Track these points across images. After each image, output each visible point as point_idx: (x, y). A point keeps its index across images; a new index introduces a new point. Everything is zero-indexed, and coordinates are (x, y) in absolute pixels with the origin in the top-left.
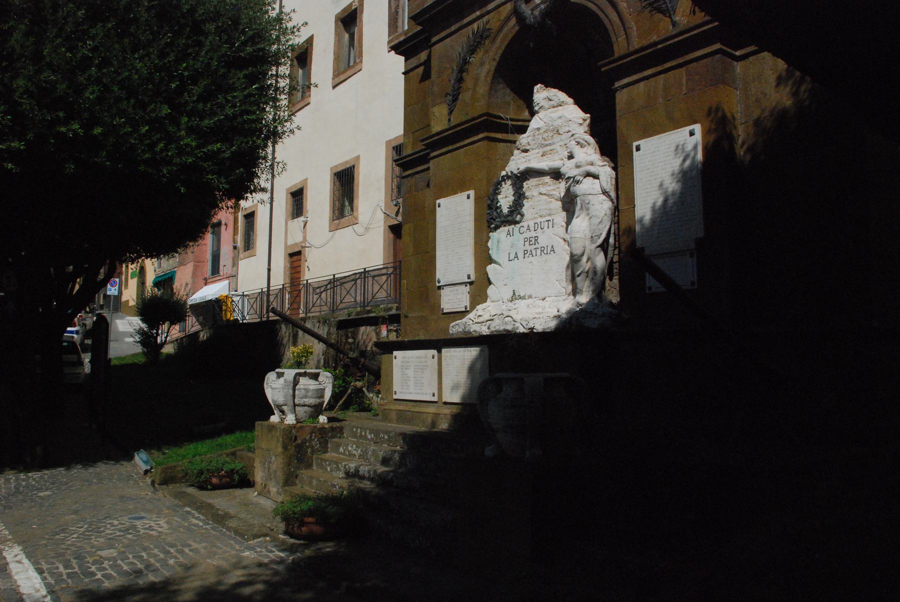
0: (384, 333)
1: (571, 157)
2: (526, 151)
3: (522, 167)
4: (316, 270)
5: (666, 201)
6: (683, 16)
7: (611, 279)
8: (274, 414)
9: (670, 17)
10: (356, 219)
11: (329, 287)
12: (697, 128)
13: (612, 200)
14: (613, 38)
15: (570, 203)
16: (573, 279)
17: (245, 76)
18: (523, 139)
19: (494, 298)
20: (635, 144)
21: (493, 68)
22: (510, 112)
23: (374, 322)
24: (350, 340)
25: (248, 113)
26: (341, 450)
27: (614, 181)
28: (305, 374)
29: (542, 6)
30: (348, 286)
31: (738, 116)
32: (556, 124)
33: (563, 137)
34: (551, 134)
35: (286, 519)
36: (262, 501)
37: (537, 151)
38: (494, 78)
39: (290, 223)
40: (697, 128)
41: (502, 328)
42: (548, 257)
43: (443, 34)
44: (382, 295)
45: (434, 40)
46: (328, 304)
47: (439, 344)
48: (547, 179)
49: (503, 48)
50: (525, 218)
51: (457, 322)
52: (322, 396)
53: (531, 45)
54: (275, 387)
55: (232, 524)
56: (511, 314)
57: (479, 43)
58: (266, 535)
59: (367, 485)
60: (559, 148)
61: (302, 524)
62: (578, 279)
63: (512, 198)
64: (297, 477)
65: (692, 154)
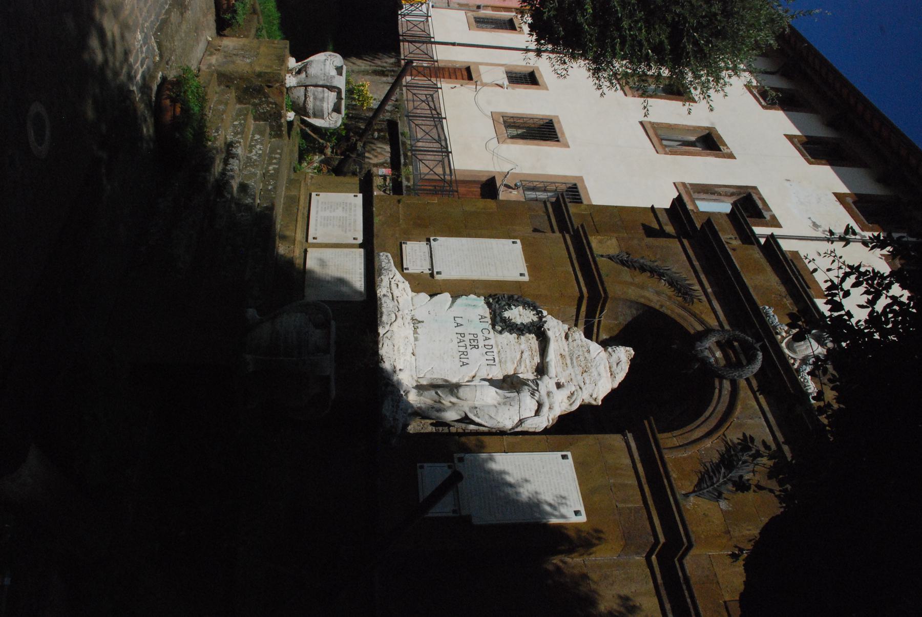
0: (383, 171)
1: (559, 386)
2: (567, 337)
3: (550, 334)
4: (452, 97)
5: (511, 485)
6: (694, 504)
7: (432, 424)
8: (297, 62)
9: (694, 491)
10: (504, 142)
11: (434, 112)
12: (583, 518)
13: (513, 428)
14: (676, 433)
15: (510, 384)
16: (434, 386)
17: (661, 42)
18: (578, 335)
19: (415, 299)
20: (569, 454)
21: (652, 305)
22: (607, 321)
23: (395, 164)
24: (376, 134)
25: (623, 43)
26: (257, 137)
27: (533, 430)
28: (339, 98)
29: (712, 360)
30: (434, 133)
31: (592, 558)
32: (593, 370)
33: (579, 377)
34: (583, 364)
35: (179, 83)
36: (202, 46)
37: (567, 349)
38: (644, 305)
39: (503, 69)
40: (583, 518)
41: (384, 310)
42: (457, 359)
43: (690, 252)
44: (423, 169)
45: (685, 242)
46: (415, 111)
47: (369, 245)
48: (537, 359)
49: (673, 316)
50: (498, 335)
51: (392, 261)
52: (315, 116)
53: (675, 346)
54: (326, 64)
55: (174, 17)
56: (399, 319)
57: (679, 291)
58: (161, 56)
59: (218, 167)
60: (568, 372)
61: (174, 101)
62: (433, 392)
63: (518, 321)
64: (227, 86)
65: (556, 513)
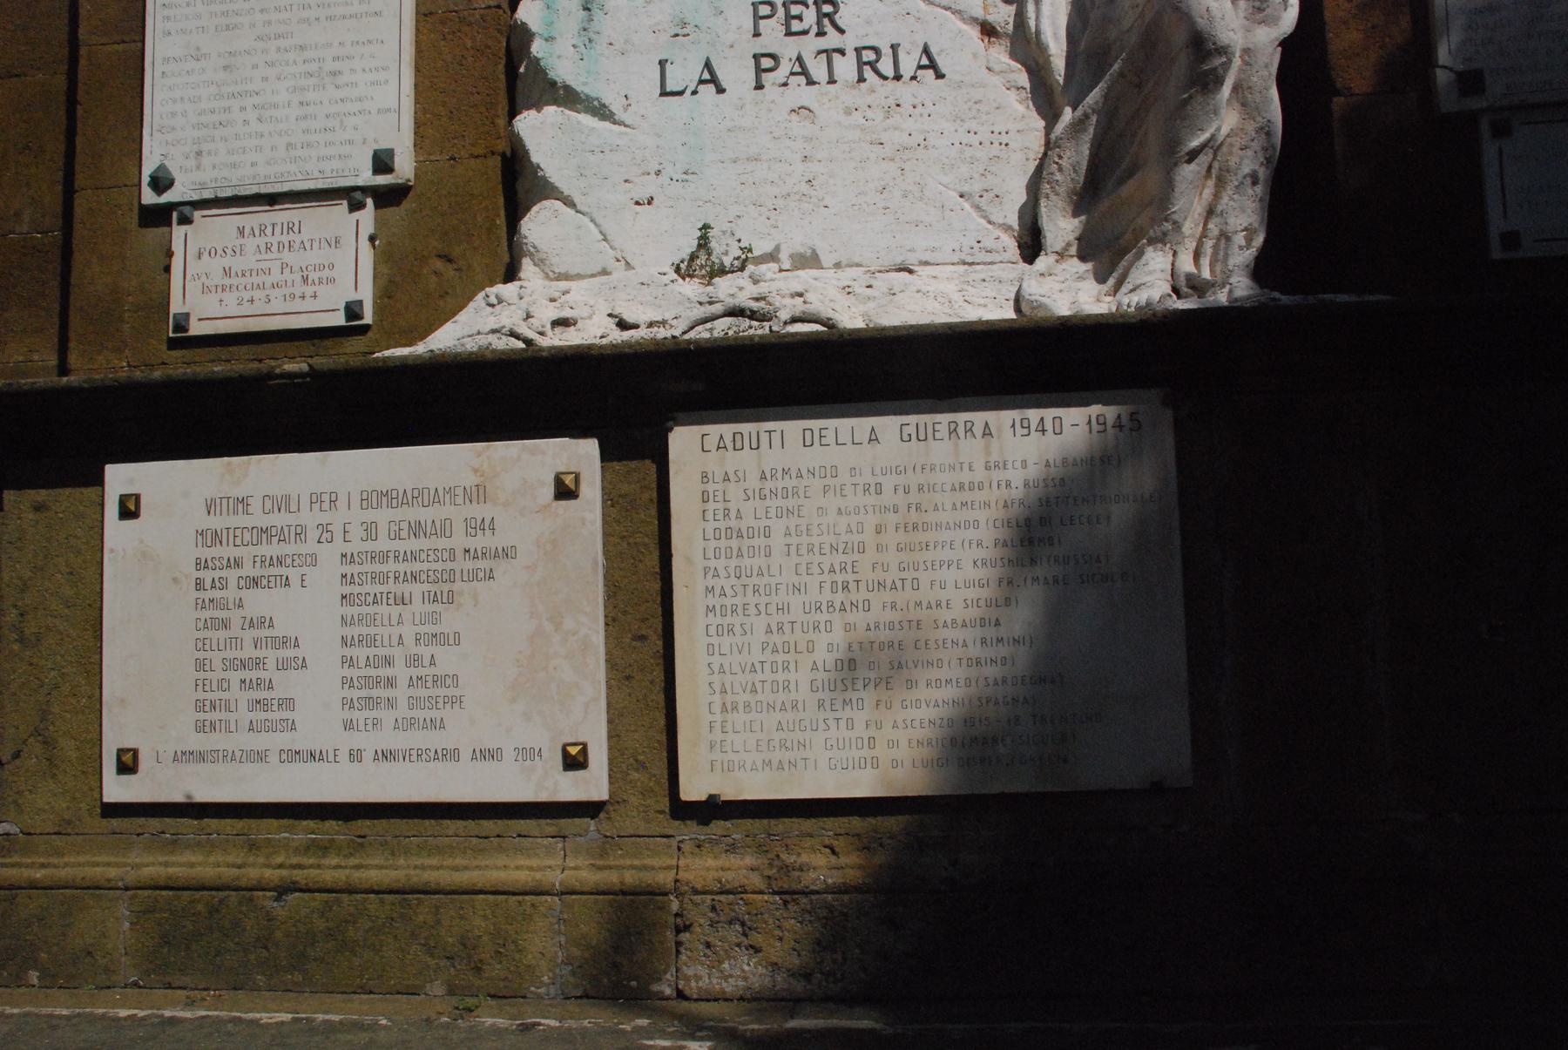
42: (903, 90)
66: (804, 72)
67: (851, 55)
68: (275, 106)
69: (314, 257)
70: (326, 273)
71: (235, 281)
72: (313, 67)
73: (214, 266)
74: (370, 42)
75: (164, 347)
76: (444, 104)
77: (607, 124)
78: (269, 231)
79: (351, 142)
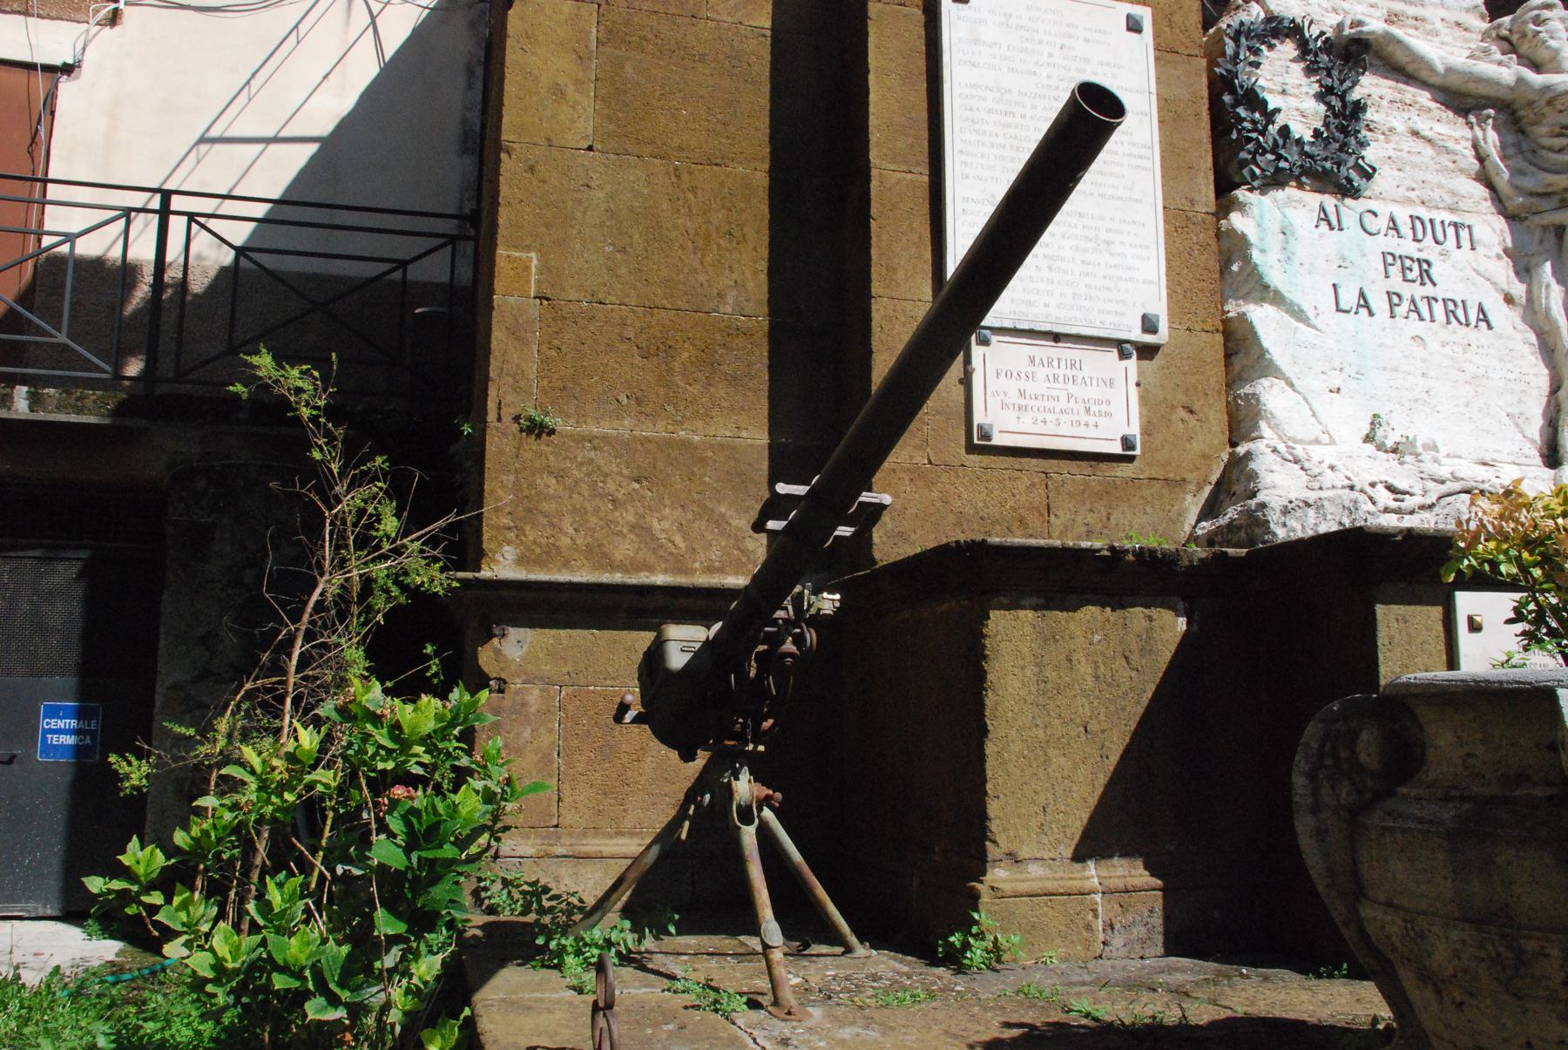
42: (1471, 334)
48: (1424, 97)
66: (1417, 311)
67: (1441, 302)
68: (1062, 259)
69: (1093, 392)
70: (1104, 408)
71: (1030, 403)
72: (1091, 233)
73: (1013, 386)
74: (1134, 223)
75: (963, 451)
76: (1180, 284)
77: (1301, 325)
78: (1055, 363)
79: (1124, 303)
